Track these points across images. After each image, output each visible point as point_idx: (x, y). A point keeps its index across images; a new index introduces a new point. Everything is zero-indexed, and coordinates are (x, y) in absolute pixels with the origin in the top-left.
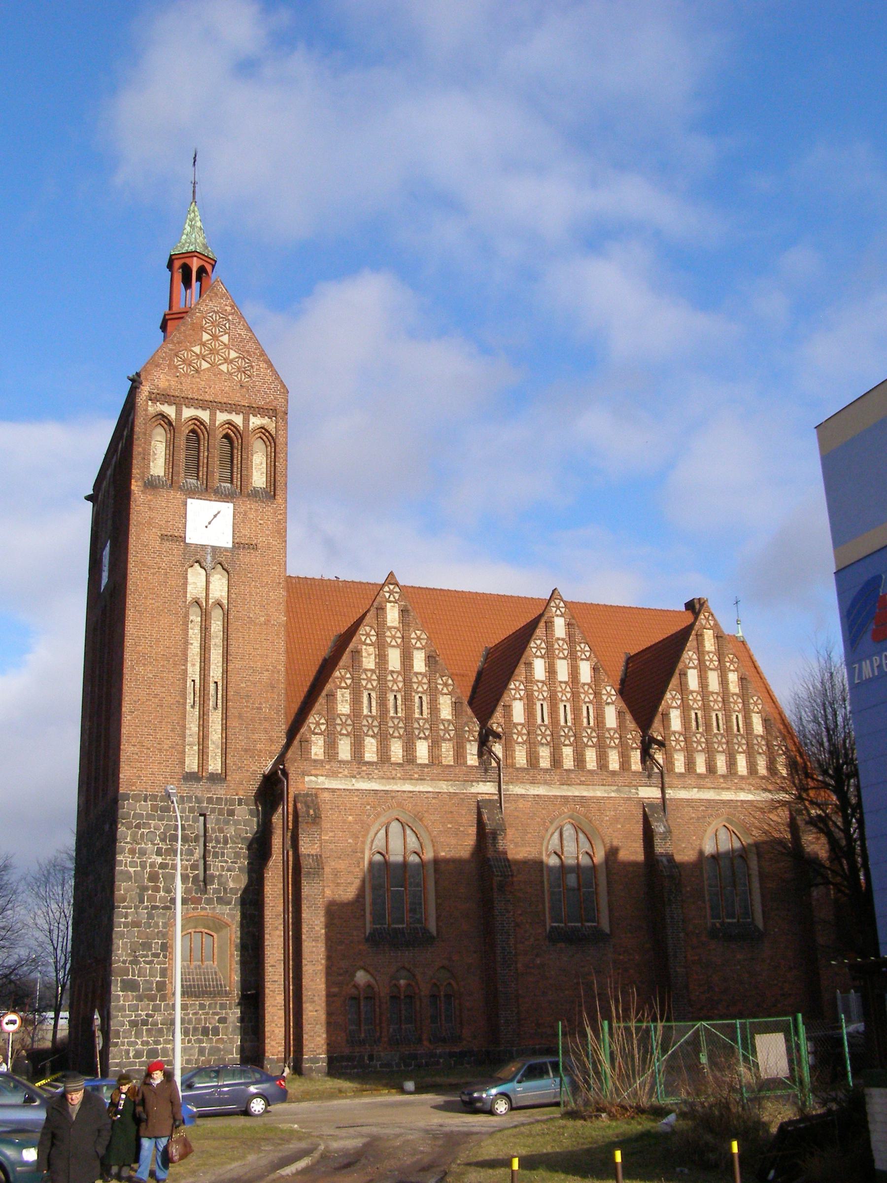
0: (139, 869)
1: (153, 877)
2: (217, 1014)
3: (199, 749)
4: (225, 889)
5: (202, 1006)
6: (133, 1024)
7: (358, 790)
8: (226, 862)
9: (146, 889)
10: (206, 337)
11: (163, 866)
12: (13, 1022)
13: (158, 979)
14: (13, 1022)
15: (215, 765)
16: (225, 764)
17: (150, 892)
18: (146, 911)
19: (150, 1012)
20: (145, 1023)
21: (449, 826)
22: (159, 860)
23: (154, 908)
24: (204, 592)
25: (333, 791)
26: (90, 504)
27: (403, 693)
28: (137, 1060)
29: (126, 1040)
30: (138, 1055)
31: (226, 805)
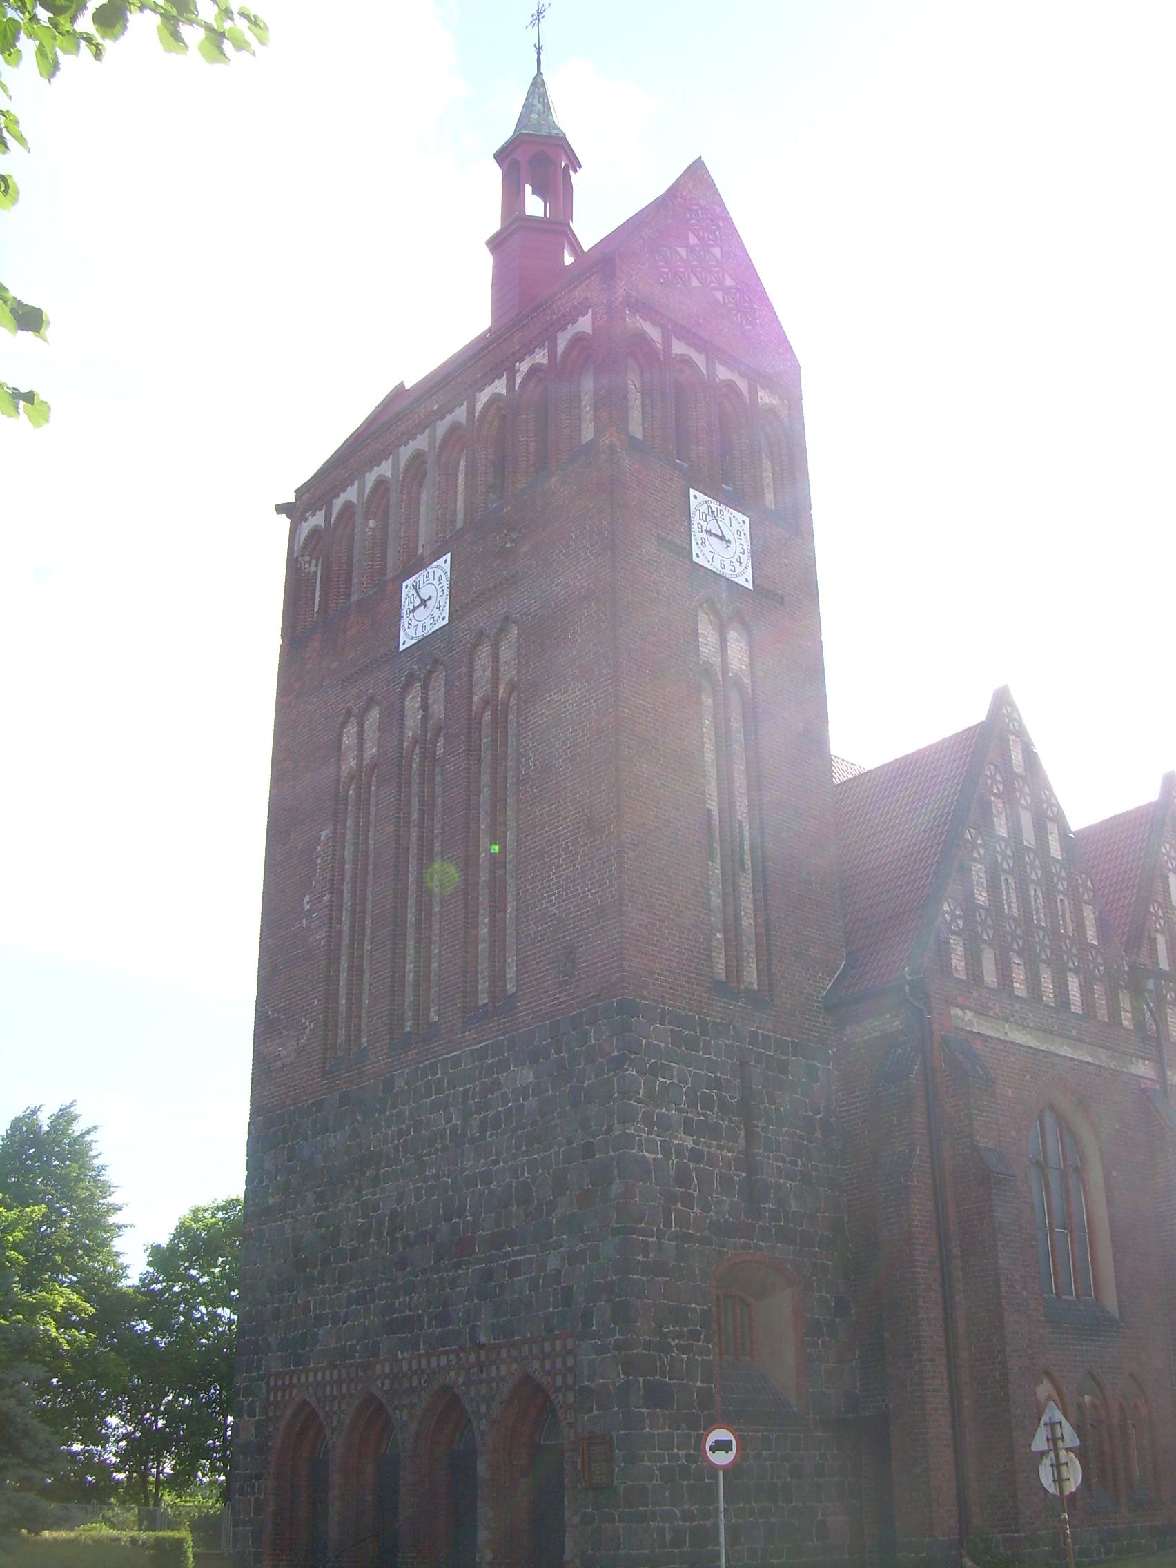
0: (660, 1156)
1: (683, 1178)
3: (726, 940)
7: (1013, 1043)
8: (784, 1161)
10: (693, 240)
11: (696, 1156)
12: (722, 1446)
13: (699, 1384)
14: (722, 1446)
15: (751, 975)
16: (765, 972)
17: (679, 1206)
18: (674, 1243)
19: (692, 1452)
22: (689, 1143)
23: (686, 1238)
24: (718, 655)
25: (985, 1038)
26: (284, 522)
27: (1044, 888)
29: (657, 1508)
31: (775, 1051)
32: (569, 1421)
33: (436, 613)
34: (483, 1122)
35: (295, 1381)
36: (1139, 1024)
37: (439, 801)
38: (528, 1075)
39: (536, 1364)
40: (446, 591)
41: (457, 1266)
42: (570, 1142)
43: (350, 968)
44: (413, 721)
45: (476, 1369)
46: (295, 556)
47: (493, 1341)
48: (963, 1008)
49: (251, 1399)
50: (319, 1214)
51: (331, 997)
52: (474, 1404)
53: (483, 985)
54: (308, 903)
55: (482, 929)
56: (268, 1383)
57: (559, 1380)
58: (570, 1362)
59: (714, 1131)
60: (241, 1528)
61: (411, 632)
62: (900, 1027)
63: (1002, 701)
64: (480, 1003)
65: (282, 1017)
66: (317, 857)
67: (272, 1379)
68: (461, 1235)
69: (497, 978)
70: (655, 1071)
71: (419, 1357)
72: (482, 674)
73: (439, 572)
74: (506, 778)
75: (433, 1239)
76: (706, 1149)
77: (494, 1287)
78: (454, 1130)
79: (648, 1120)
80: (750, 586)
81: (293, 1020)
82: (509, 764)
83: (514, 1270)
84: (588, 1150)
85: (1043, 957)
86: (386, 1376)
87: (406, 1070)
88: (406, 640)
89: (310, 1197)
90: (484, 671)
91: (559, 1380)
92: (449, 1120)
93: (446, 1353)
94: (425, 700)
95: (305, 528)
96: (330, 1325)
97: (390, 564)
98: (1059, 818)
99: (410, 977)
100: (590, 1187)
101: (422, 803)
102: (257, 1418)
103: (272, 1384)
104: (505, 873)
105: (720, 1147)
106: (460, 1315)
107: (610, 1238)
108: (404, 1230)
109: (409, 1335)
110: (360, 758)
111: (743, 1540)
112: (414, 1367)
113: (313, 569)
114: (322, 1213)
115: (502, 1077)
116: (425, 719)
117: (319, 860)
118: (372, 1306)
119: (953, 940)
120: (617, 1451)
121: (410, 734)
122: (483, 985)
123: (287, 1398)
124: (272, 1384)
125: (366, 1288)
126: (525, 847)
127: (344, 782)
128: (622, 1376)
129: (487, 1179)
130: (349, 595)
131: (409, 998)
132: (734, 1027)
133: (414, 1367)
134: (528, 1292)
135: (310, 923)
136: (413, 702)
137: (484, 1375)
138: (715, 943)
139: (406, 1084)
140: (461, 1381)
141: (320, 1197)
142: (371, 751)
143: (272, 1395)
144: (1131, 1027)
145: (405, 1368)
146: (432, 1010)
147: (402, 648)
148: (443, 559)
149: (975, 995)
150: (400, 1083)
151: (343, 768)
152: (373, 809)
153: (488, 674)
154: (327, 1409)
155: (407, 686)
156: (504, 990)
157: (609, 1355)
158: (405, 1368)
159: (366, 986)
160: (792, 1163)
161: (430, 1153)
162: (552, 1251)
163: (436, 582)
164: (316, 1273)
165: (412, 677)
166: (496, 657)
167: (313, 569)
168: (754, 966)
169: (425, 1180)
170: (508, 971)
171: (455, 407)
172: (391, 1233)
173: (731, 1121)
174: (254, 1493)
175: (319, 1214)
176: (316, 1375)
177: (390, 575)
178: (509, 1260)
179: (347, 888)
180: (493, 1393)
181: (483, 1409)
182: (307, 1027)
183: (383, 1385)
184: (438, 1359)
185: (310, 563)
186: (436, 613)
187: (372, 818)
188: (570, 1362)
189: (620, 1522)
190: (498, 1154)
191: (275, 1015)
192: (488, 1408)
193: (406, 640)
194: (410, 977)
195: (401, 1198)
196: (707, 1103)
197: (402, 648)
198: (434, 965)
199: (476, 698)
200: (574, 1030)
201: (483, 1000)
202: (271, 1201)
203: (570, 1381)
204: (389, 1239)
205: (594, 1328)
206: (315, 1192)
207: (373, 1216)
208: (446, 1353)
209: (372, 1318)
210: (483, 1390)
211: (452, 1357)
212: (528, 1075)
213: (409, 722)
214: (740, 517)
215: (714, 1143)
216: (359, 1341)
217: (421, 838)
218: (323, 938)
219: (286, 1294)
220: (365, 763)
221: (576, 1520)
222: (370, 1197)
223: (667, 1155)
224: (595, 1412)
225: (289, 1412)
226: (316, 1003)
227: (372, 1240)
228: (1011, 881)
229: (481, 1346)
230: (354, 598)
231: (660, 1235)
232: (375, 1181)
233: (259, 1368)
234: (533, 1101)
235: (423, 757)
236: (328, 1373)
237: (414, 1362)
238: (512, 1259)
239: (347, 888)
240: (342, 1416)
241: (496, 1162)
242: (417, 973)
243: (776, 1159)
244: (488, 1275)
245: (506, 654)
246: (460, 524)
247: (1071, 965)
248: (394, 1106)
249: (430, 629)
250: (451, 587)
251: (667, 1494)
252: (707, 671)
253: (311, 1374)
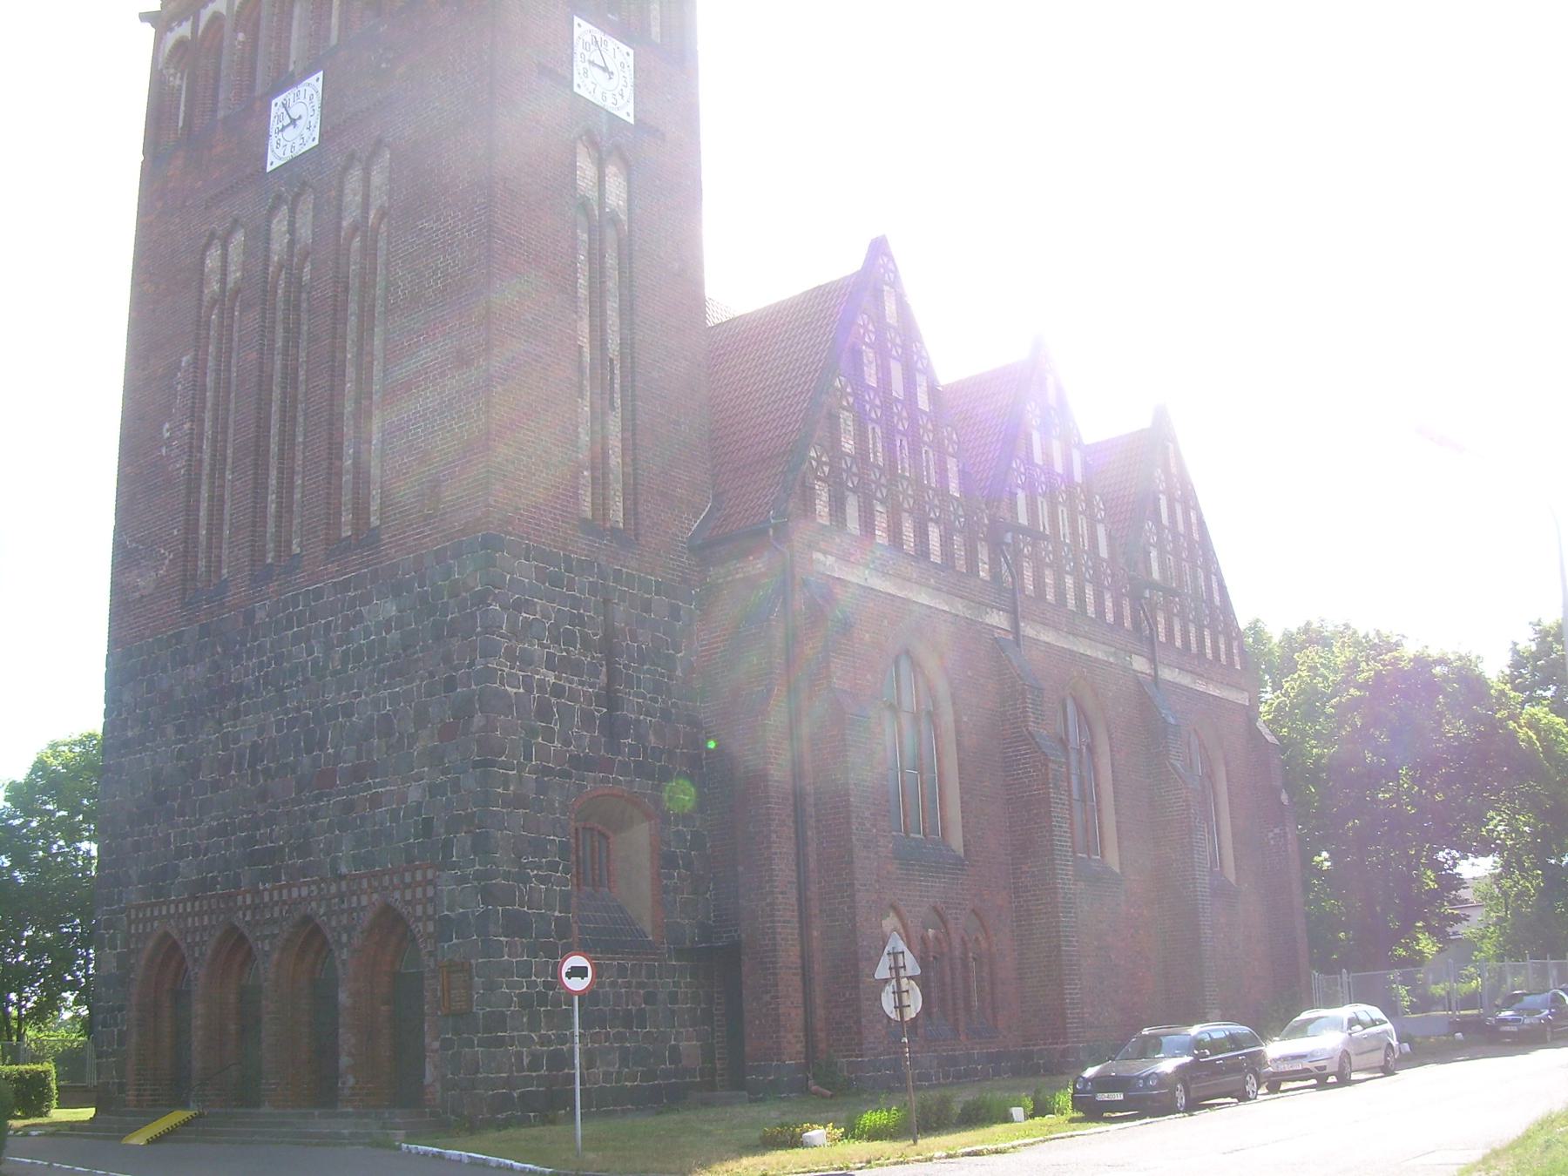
0: (521, 690)
1: (544, 712)
2: (641, 985)
3: (593, 478)
4: (645, 748)
5: (622, 970)
6: (526, 1002)
8: (644, 697)
9: (533, 732)
11: (558, 691)
12: (578, 972)
13: (557, 914)
14: (578, 972)
15: (617, 514)
16: (631, 511)
18: (534, 777)
19: (549, 979)
20: (542, 999)
21: (969, 673)
22: (551, 678)
23: (547, 771)
24: (596, 189)
26: (148, 32)
27: (910, 439)
28: (534, 1074)
29: (516, 1034)
30: (535, 1064)
32: (429, 949)
33: (306, 133)
34: (345, 653)
35: (156, 913)
36: (995, 575)
37: (305, 328)
38: (391, 609)
39: (397, 895)
40: (318, 112)
41: (318, 798)
42: (432, 675)
43: (211, 498)
44: (279, 244)
45: (337, 900)
46: (159, 67)
47: (354, 872)
48: (825, 553)
49: (112, 931)
50: (179, 746)
51: (191, 528)
52: (335, 934)
53: (346, 517)
54: (168, 431)
55: (346, 461)
56: (128, 916)
57: (419, 909)
58: (430, 892)
59: (575, 668)
60: (104, 1060)
61: (279, 152)
62: (763, 570)
63: (878, 248)
64: (344, 535)
65: (141, 547)
66: (177, 384)
67: (133, 912)
68: (323, 767)
70: (518, 606)
71: (281, 888)
72: (352, 199)
73: (310, 91)
74: (374, 306)
75: (294, 771)
76: (568, 685)
77: (355, 819)
78: (315, 662)
79: (511, 655)
80: (631, 120)
81: (151, 550)
82: (378, 292)
83: (375, 801)
84: (450, 685)
85: (906, 506)
86: (248, 908)
87: (268, 602)
88: (274, 160)
89: (170, 730)
90: (355, 195)
91: (419, 909)
92: (310, 653)
93: (308, 884)
94: (292, 224)
95: (171, 39)
97: (258, 81)
98: (928, 371)
99: (272, 508)
100: (452, 720)
101: (287, 330)
102: (119, 950)
103: (133, 917)
104: (371, 404)
105: (582, 683)
106: (322, 846)
107: (471, 770)
108: (265, 762)
109: (270, 867)
110: (223, 282)
111: (598, 1064)
112: (276, 898)
113: (178, 82)
116: (292, 243)
117: (180, 387)
118: (233, 838)
119: (818, 485)
120: (476, 979)
121: (276, 258)
122: (346, 517)
123: (148, 930)
124: (133, 917)
125: (227, 820)
127: (207, 307)
128: (481, 906)
129: (348, 711)
130: (214, 111)
131: (271, 528)
132: (599, 564)
133: (276, 898)
134: (388, 824)
135: (171, 450)
136: (279, 226)
137: (345, 906)
138: (582, 481)
139: (267, 616)
140: (322, 911)
141: (180, 729)
142: (235, 275)
143: (133, 927)
144: (988, 578)
145: (267, 899)
146: (294, 542)
147: (269, 169)
148: (315, 77)
149: (838, 540)
150: (261, 615)
151: (206, 291)
152: (236, 336)
153: (358, 198)
154: (189, 941)
155: (273, 210)
156: (368, 522)
157: (469, 885)
158: (267, 899)
159: (227, 517)
160: (652, 699)
161: (290, 686)
162: (413, 783)
163: (307, 101)
164: (176, 806)
165: (279, 199)
166: (366, 180)
167: (178, 82)
168: (620, 505)
169: (286, 712)
170: (372, 503)
172: (252, 765)
173: (593, 658)
174: (116, 1025)
175: (179, 746)
176: (177, 907)
177: (259, 91)
178: (370, 792)
179: (208, 415)
180: (355, 922)
181: (344, 938)
182: (166, 558)
183: (244, 915)
184: (299, 891)
185: (174, 75)
186: (306, 133)
187: (235, 344)
188: (430, 892)
189: (478, 1046)
190: (360, 687)
191: (134, 545)
192: (350, 937)
193: (274, 160)
194: (272, 508)
195: (262, 729)
196: (570, 640)
197: (269, 169)
198: (297, 496)
199: (345, 224)
200: (437, 564)
201: (347, 532)
202: (130, 734)
203: (430, 911)
204: (249, 772)
205: (454, 859)
206: (175, 725)
207: (233, 748)
208: (308, 884)
209: (233, 850)
211: (313, 888)
212: (391, 609)
213: (275, 247)
214: (625, 48)
215: (576, 678)
216: (219, 872)
217: (285, 366)
218: (184, 467)
219: (147, 826)
220: (228, 287)
221: (436, 1045)
222: (230, 729)
223: (529, 690)
224: (455, 941)
225: (150, 944)
226: (176, 533)
227: (233, 772)
228: (878, 430)
229: (342, 877)
230: (221, 114)
231: (521, 768)
232: (236, 713)
233: (120, 901)
234: (395, 634)
235: (289, 283)
236: (189, 904)
237: (276, 893)
238: (374, 791)
239: (208, 415)
240: (204, 947)
241: (358, 695)
242: (280, 504)
243: (637, 695)
244: (349, 807)
245: (377, 178)
246: (334, 41)
247: (932, 515)
248: (255, 639)
249: (299, 150)
250: (322, 107)
251: (525, 1020)
252: (584, 205)
253: (172, 906)
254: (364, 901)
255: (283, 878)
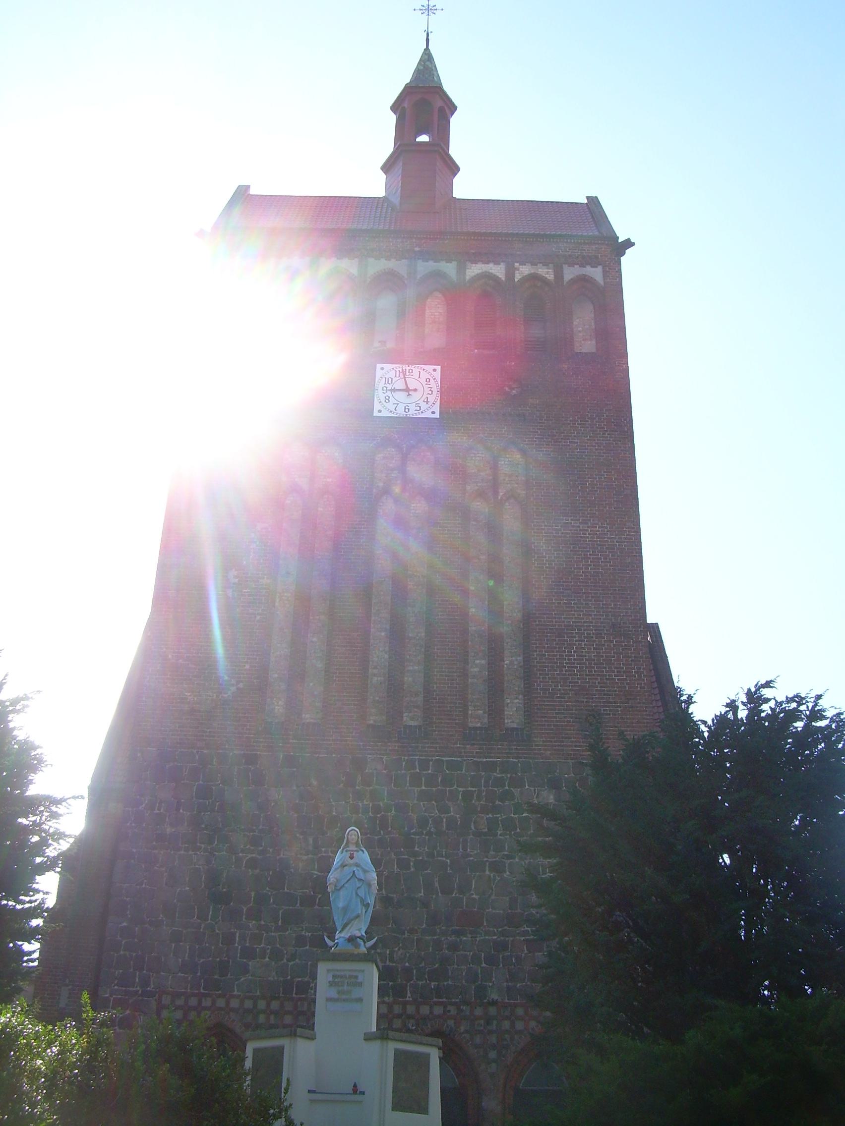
45: (482, 1022)
69: (495, 710)
71: (405, 1004)
96: (267, 959)
114: (254, 855)
115: (516, 792)
126: (539, 621)
140: (462, 1029)
171: (442, 260)
175: (250, 856)
180: (505, 1043)
181: (493, 1055)
184: (431, 1007)
199: (468, 488)
210: (493, 1039)
249: (413, 412)
254: (519, 1025)
255: (409, 995)
